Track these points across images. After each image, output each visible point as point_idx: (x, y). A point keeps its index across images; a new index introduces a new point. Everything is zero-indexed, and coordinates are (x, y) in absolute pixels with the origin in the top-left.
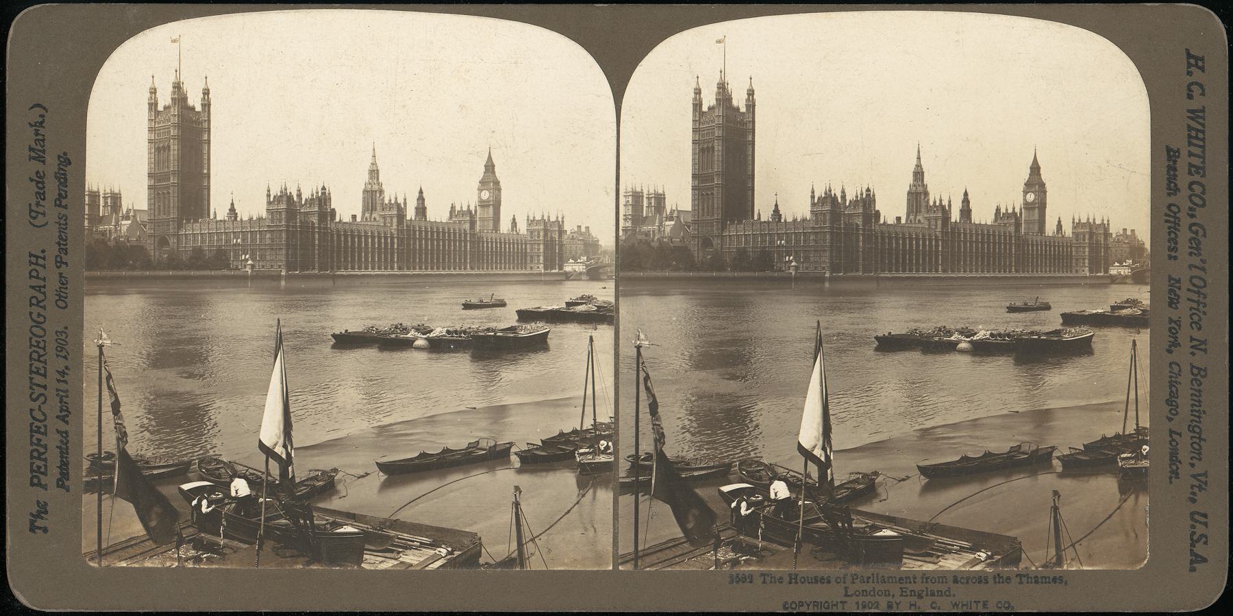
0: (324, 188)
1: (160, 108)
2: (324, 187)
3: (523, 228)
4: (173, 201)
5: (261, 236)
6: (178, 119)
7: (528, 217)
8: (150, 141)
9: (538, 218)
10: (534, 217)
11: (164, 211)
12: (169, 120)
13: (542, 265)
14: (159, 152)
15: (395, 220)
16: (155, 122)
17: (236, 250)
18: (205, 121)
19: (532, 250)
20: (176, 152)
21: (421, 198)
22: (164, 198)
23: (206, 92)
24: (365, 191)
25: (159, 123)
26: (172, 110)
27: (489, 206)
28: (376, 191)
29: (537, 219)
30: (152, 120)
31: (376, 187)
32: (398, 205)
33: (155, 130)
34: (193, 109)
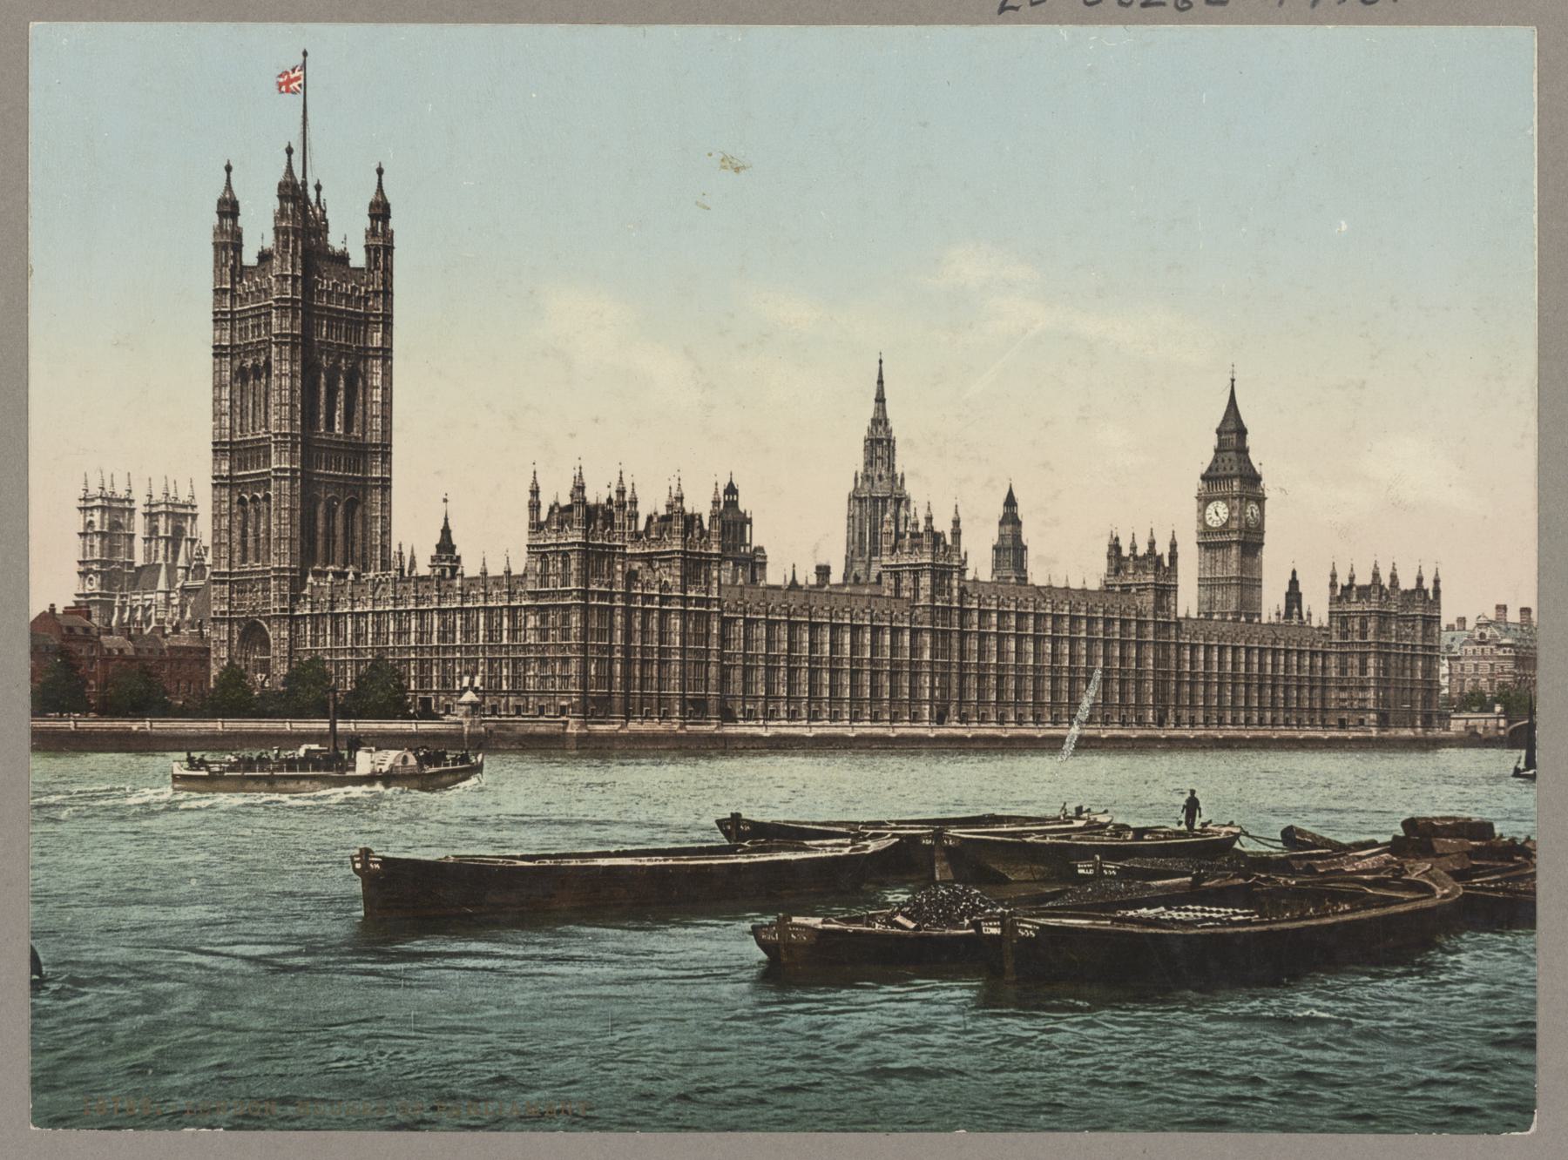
0: (731, 490)
1: (250, 258)
2: (731, 484)
3: (1317, 607)
4: (279, 521)
5: (515, 624)
6: (293, 285)
7: (1334, 576)
8: (219, 351)
9: (1364, 579)
10: (1352, 578)
11: (257, 549)
12: (267, 293)
13: (1373, 716)
14: (245, 381)
15: (925, 581)
16: (232, 296)
17: (445, 661)
18: (376, 293)
19: (1343, 671)
20: (286, 382)
21: (1011, 517)
22: (257, 511)
23: (380, 211)
24: (856, 498)
25: (243, 300)
26: (276, 262)
27: (1226, 545)
28: (884, 499)
29: (1359, 582)
30: (225, 291)
31: (881, 490)
32: (937, 538)
33: (232, 320)
34: (343, 258)
